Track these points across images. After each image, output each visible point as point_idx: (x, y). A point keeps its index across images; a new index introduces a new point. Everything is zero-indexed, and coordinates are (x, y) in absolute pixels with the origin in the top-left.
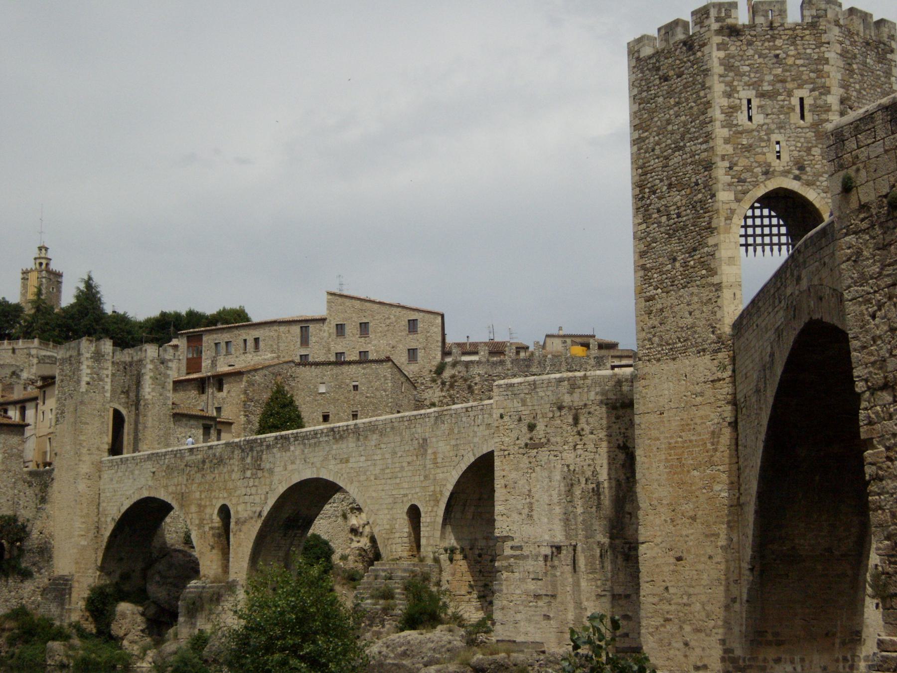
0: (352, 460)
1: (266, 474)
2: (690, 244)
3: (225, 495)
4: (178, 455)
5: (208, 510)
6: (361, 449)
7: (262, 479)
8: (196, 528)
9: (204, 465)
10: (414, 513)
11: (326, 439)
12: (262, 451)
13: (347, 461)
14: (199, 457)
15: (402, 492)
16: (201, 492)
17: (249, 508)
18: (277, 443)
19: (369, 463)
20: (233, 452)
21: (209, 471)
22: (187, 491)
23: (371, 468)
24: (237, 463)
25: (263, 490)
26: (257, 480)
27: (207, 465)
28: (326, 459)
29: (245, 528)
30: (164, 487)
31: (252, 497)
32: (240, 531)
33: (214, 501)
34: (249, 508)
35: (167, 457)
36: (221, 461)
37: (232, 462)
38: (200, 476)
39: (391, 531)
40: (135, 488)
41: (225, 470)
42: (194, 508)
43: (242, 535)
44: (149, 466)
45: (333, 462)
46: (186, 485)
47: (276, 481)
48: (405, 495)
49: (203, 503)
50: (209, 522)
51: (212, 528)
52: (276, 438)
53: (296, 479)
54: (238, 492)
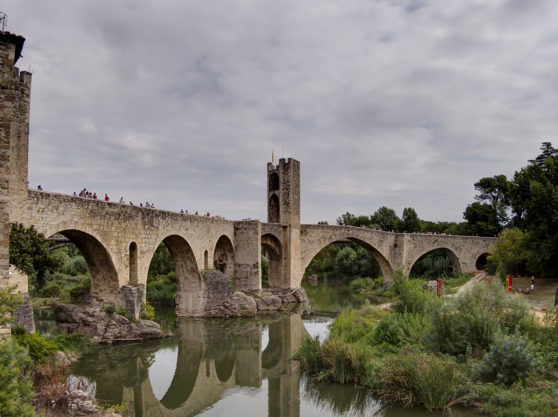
0: (189, 230)
1: (156, 229)
2: (297, 207)
3: (134, 237)
4: (100, 205)
5: (124, 244)
6: (192, 226)
7: (153, 231)
8: (116, 255)
9: (120, 216)
10: (206, 252)
11: (180, 218)
12: (153, 217)
13: (188, 230)
14: (116, 210)
15: (204, 245)
16: (118, 232)
17: (147, 245)
18: (160, 214)
19: (195, 232)
20: (138, 213)
21: (123, 221)
22: (108, 230)
23: (195, 235)
24: (140, 220)
25: (154, 237)
26: (151, 231)
27: (122, 217)
28: (180, 227)
29: (145, 256)
30: (88, 224)
31: (149, 240)
32: (143, 257)
33: (127, 239)
34: (147, 245)
35: (91, 204)
36: (130, 217)
37: (137, 218)
38: (117, 223)
39: (200, 259)
40: (60, 221)
41: (133, 222)
42: (113, 242)
43: (144, 259)
44: (74, 207)
45: (183, 229)
46: (107, 227)
47: (160, 234)
48: (204, 246)
49: (120, 240)
50: (124, 251)
51: (126, 255)
52: (160, 212)
53: (169, 234)
54: (141, 237)
